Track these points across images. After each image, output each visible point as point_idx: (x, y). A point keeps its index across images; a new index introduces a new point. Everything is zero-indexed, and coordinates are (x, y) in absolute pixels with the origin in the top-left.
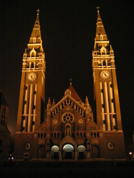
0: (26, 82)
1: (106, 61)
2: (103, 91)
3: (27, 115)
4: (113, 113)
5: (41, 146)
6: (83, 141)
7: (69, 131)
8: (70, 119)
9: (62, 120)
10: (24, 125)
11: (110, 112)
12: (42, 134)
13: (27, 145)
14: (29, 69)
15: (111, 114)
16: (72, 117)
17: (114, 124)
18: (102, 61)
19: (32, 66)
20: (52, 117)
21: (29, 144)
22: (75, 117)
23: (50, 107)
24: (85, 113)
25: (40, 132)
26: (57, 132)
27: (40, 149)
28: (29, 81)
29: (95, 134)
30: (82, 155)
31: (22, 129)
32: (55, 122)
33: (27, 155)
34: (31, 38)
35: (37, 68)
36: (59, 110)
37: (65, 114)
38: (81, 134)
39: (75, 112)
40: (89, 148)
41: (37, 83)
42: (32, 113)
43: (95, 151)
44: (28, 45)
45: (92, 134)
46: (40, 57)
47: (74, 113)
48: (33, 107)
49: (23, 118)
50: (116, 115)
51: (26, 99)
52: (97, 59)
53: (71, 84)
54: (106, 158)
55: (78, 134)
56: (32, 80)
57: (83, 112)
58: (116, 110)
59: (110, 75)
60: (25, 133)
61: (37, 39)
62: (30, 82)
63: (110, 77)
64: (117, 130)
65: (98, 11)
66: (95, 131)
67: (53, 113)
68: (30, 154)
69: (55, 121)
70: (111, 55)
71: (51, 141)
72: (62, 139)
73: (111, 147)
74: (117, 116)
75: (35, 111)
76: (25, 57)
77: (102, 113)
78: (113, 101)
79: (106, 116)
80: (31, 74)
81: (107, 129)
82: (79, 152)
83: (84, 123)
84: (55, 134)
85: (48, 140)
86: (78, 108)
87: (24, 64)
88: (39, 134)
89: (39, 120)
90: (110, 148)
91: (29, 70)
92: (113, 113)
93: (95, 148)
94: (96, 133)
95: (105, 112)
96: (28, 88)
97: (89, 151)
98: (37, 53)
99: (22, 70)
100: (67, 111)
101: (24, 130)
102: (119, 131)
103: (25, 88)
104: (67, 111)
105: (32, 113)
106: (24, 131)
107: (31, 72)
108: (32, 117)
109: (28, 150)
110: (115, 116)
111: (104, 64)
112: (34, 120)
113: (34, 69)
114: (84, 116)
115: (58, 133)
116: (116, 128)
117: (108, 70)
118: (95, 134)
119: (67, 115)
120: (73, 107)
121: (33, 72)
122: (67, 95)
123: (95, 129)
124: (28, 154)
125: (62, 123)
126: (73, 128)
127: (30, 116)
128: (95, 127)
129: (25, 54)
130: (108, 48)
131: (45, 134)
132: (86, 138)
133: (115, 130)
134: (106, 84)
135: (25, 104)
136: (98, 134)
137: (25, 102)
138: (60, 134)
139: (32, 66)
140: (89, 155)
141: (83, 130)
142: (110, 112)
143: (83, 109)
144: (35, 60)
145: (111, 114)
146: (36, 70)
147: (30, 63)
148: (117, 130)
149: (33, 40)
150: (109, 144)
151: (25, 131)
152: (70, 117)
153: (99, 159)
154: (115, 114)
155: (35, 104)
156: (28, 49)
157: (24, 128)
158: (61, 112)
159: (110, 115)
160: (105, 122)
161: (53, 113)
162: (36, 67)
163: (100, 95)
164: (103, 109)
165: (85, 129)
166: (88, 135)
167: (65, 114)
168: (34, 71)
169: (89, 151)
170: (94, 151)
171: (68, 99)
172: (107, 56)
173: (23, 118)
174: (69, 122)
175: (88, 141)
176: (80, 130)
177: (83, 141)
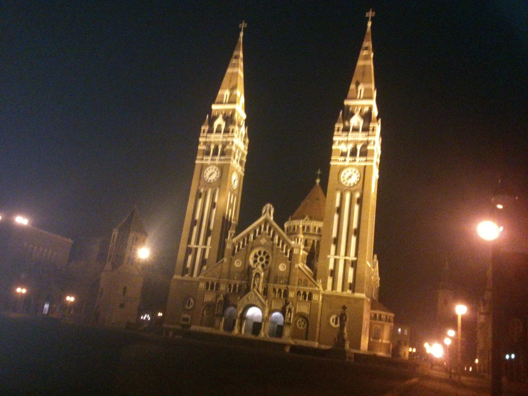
0: (202, 183)
1: (359, 147)
2: (339, 210)
3: (195, 246)
4: (352, 257)
5: (209, 306)
6: (282, 306)
7: (260, 283)
8: (264, 262)
9: (249, 262)
10: (189, 265)
11: (346, 255)
12: (213, 284)
13: (190, 301)
14: (210, 158)
15: (347, 258)
16: (268, 257)
17: (350, 280)
18: (350, 146)
19: (215, 153)
20: (233, 254)
21: (192, 300)
22: (273, 257)
23: (233, 235)
24: (291, 252)
25: (211, 279)
26: (238, 283)
27: (206, 311)
28: (206, 182)
29: (305, 293)
30: (279, 331)
31: (185, 271)
32: (238, 263)
33: (186, 320)
34: (220, 92)
35: (223, 158)
36: (248, 242)
37: (256, 251)
38: (280, 291)
39: (274, 250)
40: (290, 319)
41: (219, 186)
42: (205, 243)
43: (300, 326)
44: (214, 107)
45: (299, 293)
46: (230, 134)
47: (272, 250)
48: (208, 233)
49: (189, 251)
50: (356, 261)
51: (197, 217)
52: (340, 143)
53: (318, 181)
54: (320, 343)
55: (274, 290)
56: (212, 182)
57: (289, 251)
58: (359, 252)
59: (360, 178)
60: (190, 279)
61: (230, 95)
62: (209, 184)
63: (358, 182)
64: (353, 292)
65: (369, 24)
66: (305, 288)
67: (237, 247)
68: (191, 317)
69: (238, 262)
70: (370, 132)
71: (226, 297)
72: (241, 298)
73: (336, 323)
74: (358, 263)
75: (210, 239)
76: (204, 132)
77: (330, 254)
78: (357, 232)
79: (336, 261)
80: (211, 167)
81: (334, 287)
82: (276, 326)
83: (289, 271)
84: (235, 285)
85: (222, 296)
86: (281, 242)
87: (201, 147)
88: (207, 284)
89: (215, 256)
90: (333, 324)
91: (208, 160)
92: (352, 257)
93: (302, 321)
94: (307, 293)
95: (337, 253)
96: (203, 196)
97: (289, 324)
98: (227, 125)
99: (195, 159)
100: (260, 245)
101: (187, 274)
102: (357, 295)
103: (199, 195)
104: (260, 245)
105: (205, 243)
106: (187, 276)
107: (211, 164)
108: (204, 251)
109: (189, 310)
110: (354, 264)
111: (353, 153)
112: (207, 256)
113: (218, 158)
114: (290, 259)
115: (240, 286)
116: (352, 287)
117: (358, 168)
118: (305, 293)
119: (260, 253)
120: (272, 239)
121: (215, 164)
122: (265, 215)
123: (306, 285)
124: (189, 317)
125: (250, 267)
126: (267, 279)
127: (200, 247)
128: (307, 281)
129: (205, 128)
130: (367, 117)
131: (218, 285)
132: (286, 301)
133: (349, 292)
134: (348, 196)
135: (195, 225)
136: (311, 295)
137: (196, 221)
138: (242, 287)
139: (215, 153)
140: (287, 332)
141: (285, 284)
142: (347, 253)
143: (289, 245)
144: (221, 140)
145: (347, 258)
146: (220, 160)
147: (212, 147)
148: (353, 292)
149: (222, 96)
150: (334, 317)
151: (189, 276)
152: (264, 258)
153: (304, 343)
154: (355, 259)
155: (212, 227)
156: (212, 116)
157: (187, 269)
158: (250, 246)
159: (345, 260)
160: (333, 273)
161: (237, 247)
162: (223, 154)
163: (333, 220)
164: (333, 248)
165: (288, 283)
166: (291, 295)
167: (256, 251)
168: (217, 162)
169: (289, 324)
170: (298, 326)
171: (266, 221)
172: (361, 137)
173: (189, 251)
174: (263, 266)
175: (290, 306)
176: (278, 282)
177: (280, 306)
